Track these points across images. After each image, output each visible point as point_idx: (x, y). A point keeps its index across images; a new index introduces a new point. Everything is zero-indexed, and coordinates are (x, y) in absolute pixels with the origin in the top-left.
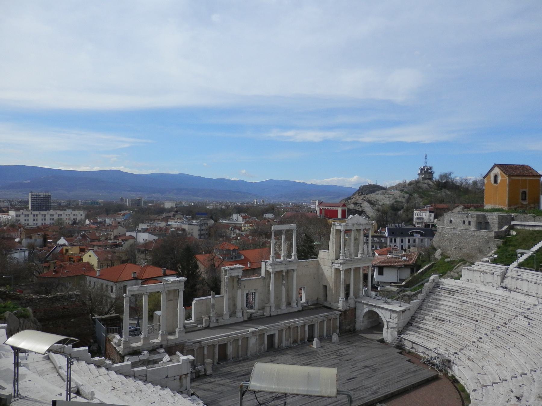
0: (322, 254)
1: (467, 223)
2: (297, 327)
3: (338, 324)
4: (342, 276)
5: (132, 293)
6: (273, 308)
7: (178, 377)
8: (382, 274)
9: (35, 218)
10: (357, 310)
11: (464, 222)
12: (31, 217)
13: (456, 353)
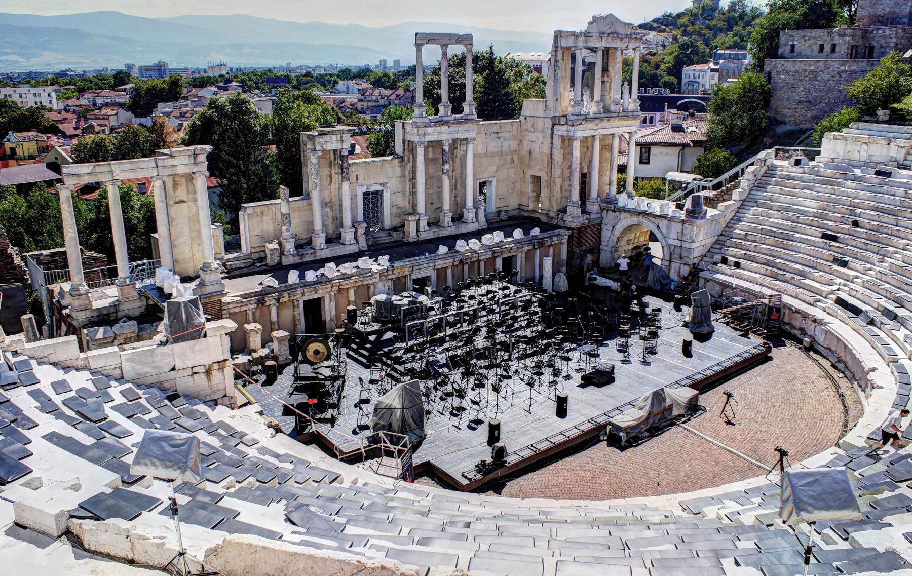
0: (530, 107)
1: (827, 48)
2: (479, 261)
3: (564, 256)
4: (577, 153)
5: (76, 181)
6: (423, 223)
7: (202, 369)
8: (648, 163)
10: (603, 227)
11: (822, 47)
13: (819, 301)
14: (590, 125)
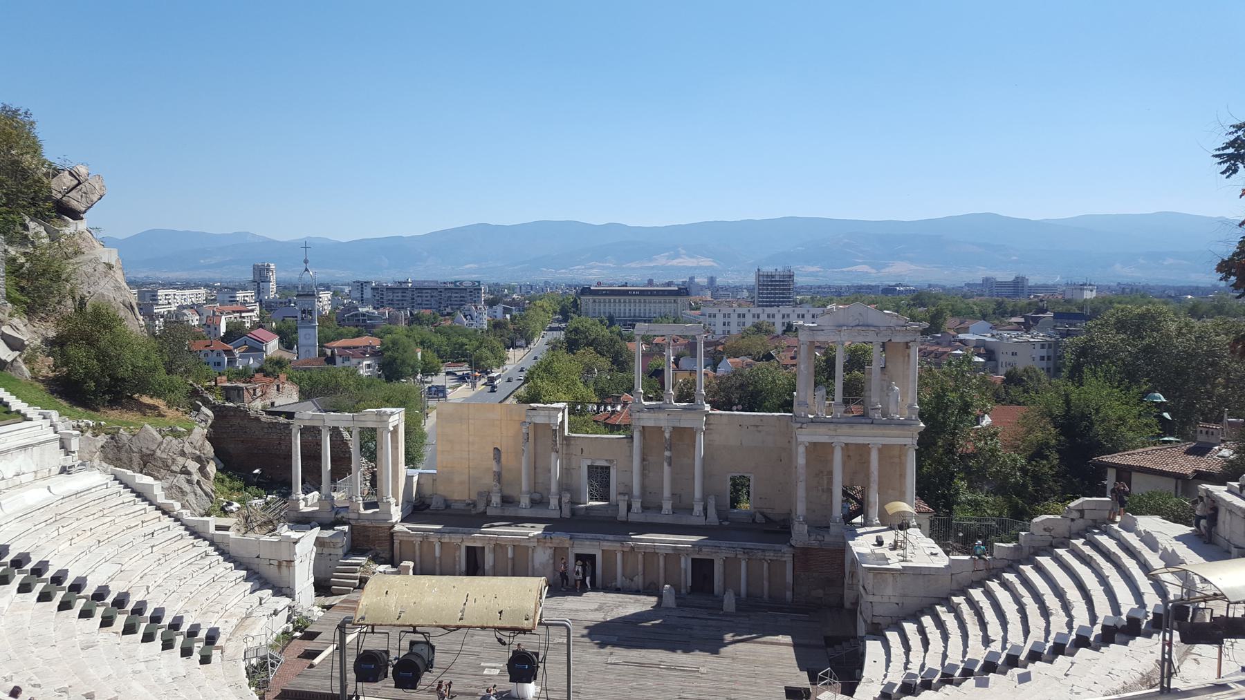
6: (636, 505)
9: (742, 320)
12: (734, 319)
14: (822, 429)
